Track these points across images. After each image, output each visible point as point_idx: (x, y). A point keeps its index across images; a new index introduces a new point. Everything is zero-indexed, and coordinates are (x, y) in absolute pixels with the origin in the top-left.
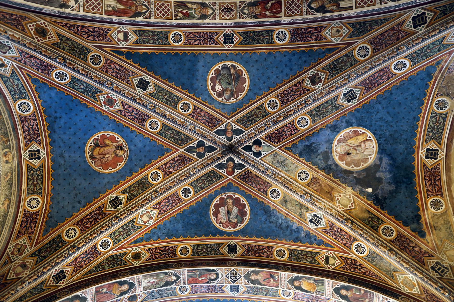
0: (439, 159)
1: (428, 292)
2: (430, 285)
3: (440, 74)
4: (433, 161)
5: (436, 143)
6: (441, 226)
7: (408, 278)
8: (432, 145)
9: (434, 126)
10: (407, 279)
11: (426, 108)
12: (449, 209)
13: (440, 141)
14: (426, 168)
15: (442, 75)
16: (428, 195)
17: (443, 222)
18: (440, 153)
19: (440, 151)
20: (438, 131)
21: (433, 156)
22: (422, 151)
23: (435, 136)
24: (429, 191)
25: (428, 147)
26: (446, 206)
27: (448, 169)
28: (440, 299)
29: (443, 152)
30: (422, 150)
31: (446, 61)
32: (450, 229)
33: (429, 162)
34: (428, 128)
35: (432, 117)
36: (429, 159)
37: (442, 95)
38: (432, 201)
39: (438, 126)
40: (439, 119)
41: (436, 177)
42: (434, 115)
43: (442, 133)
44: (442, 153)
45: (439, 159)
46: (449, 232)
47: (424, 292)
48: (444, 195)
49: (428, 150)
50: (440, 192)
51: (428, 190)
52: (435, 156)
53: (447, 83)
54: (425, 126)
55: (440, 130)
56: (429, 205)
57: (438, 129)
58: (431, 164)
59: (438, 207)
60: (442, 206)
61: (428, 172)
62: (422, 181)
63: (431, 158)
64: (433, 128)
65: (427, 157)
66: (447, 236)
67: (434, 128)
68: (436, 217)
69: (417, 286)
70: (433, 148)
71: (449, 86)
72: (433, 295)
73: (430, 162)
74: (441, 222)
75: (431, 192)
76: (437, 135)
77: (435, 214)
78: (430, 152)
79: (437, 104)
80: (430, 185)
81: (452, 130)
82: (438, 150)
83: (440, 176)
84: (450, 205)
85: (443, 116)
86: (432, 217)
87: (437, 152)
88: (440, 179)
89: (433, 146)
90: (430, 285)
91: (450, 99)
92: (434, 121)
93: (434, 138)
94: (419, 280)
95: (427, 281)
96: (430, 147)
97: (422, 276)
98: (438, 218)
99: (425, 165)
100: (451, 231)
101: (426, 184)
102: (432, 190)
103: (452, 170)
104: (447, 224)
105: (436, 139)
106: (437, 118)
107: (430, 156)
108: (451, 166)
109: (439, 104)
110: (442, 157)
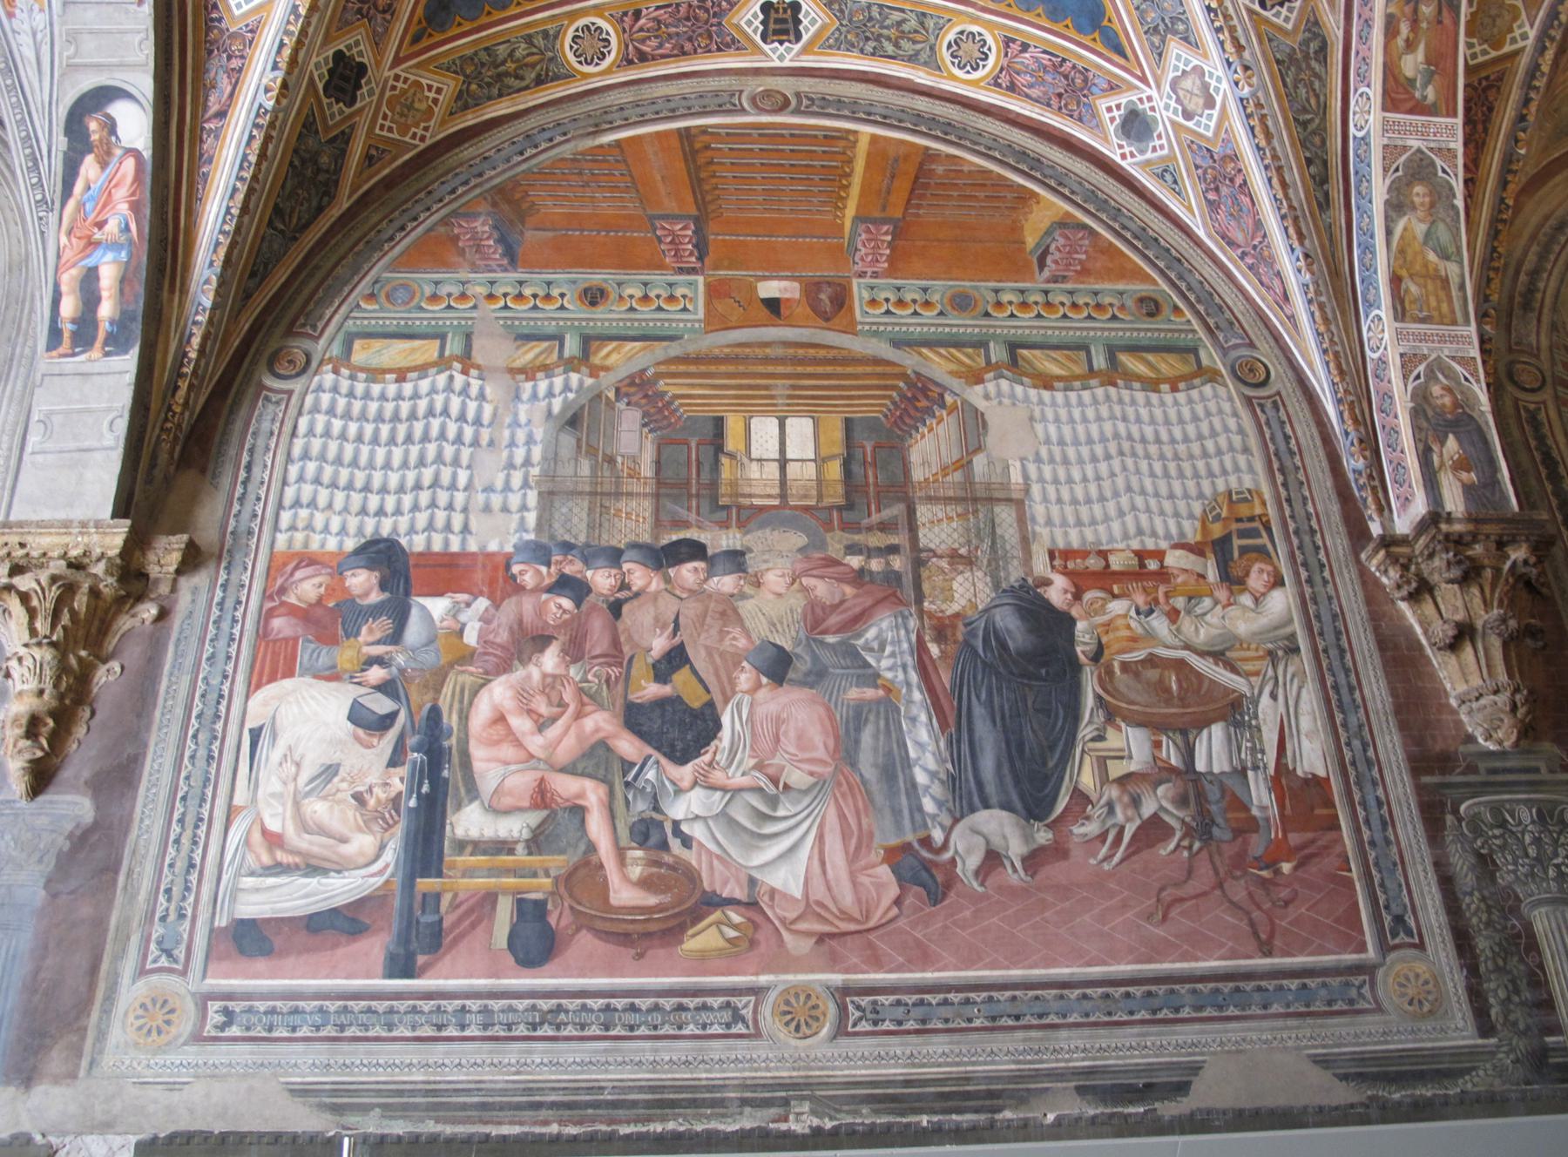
1: (1491, 94)
2: (1527, 101)
7: (1515, 18)
10: (1507, 17)
28: (1486, 130)
47: (1487, 78)
69: (1494, 54)
72: (1490, 109)
90: (1527, 101)
94: (1524, 61)
95: (1537, 88)
97: (1545, 68)
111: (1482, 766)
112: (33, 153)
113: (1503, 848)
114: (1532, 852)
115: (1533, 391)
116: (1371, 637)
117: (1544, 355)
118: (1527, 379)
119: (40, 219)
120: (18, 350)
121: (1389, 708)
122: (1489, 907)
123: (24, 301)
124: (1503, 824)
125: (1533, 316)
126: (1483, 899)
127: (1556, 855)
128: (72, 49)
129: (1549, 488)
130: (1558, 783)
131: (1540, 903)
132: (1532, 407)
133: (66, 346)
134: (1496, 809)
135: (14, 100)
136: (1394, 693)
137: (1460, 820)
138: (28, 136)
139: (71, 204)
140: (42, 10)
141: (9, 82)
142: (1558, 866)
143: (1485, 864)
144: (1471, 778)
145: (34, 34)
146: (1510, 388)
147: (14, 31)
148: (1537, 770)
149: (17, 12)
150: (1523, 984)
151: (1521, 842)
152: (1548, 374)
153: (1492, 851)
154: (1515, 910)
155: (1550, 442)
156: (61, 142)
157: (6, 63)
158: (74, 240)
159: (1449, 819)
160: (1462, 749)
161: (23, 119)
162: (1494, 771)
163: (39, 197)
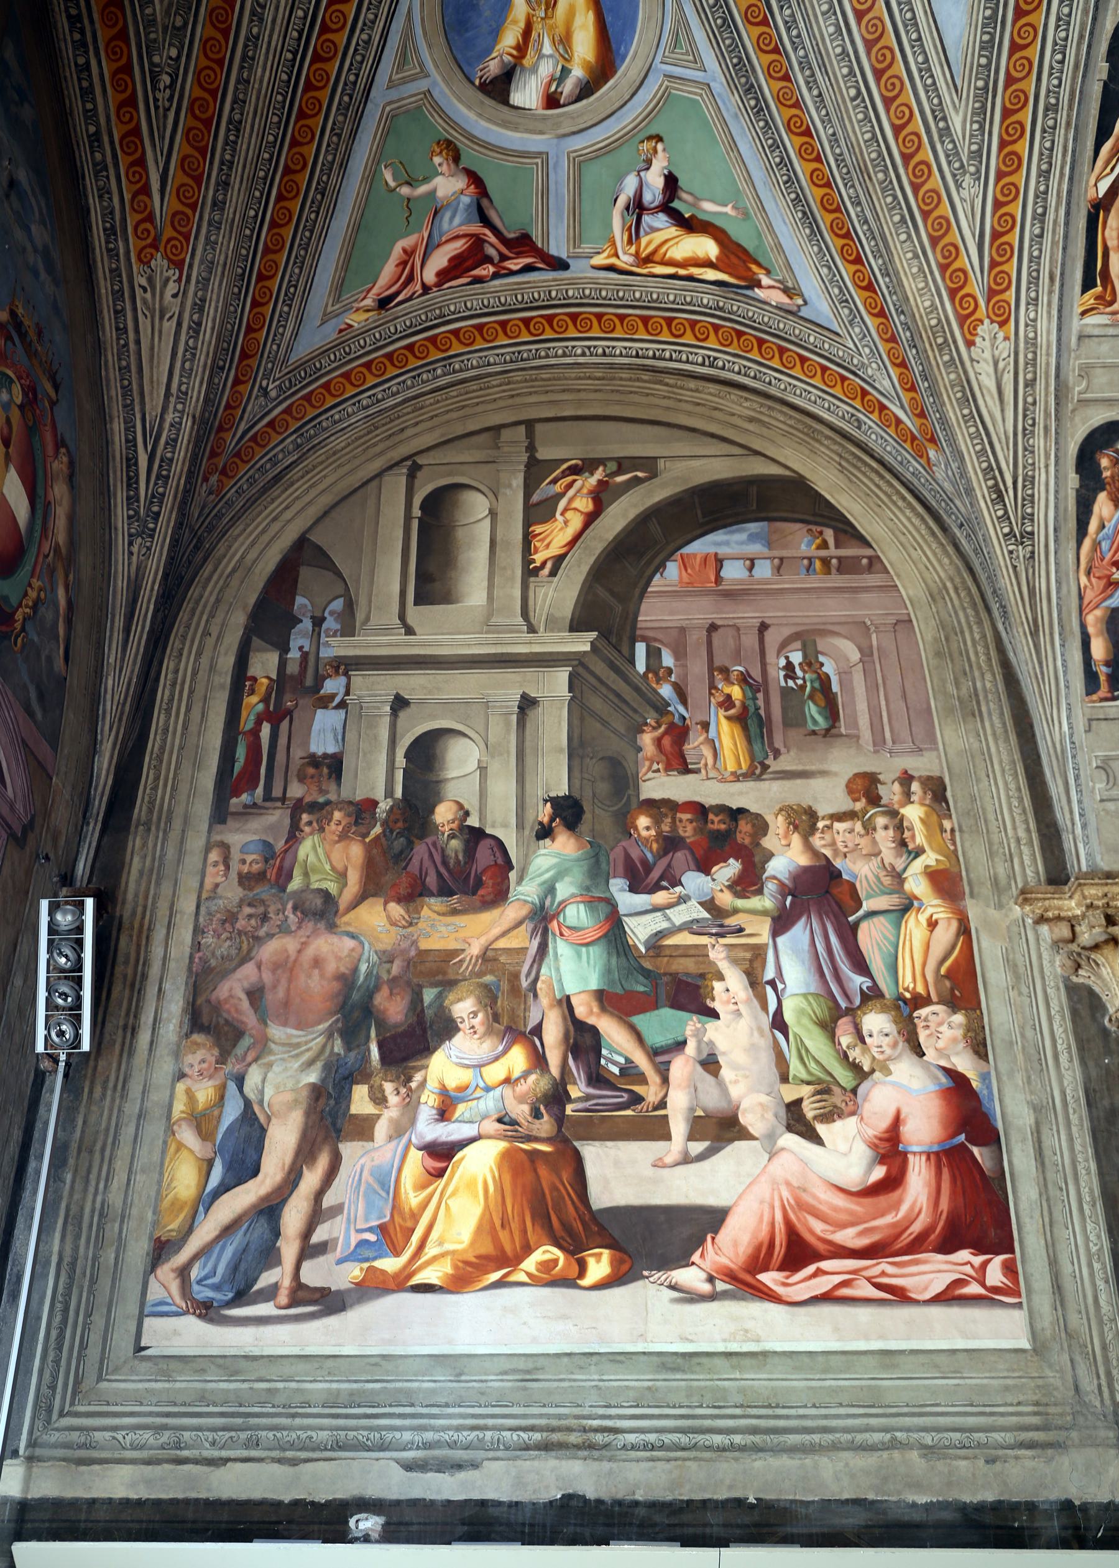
112: (996, 485)
119: (1011, 552)
120: (979, 685)
123: (962, 632)
128: (1084, 384)
133: (1104, 691)
135: (972, 430)
138: (990, 466)
139: (1087, 543)
140: (1007, 338)
141: (966, 412)
145: (996, 364)
147: (972, 360)
149: (978, 340)
156: (1073, 480)
157: (963, 391)
158: (1093, 580)
161: (984, 449)
163: (1006, 530)
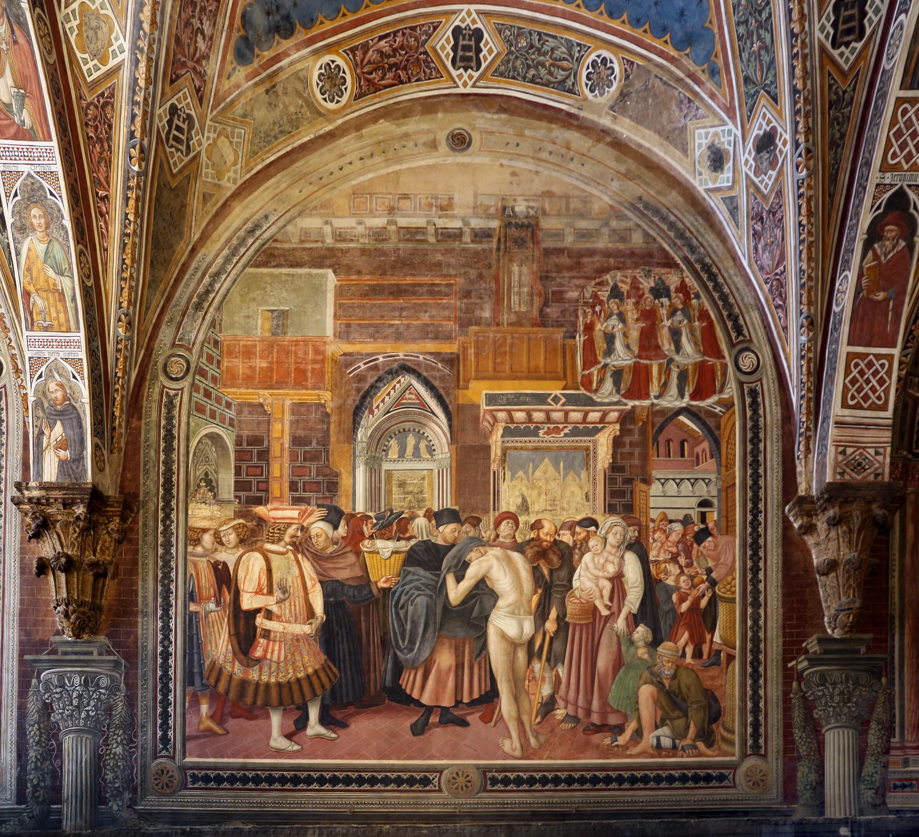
0: (454, 73)
3: (681, 75)
4: (448, 55)
5: (498, 62)
6: (281, 106)
8: (491, 47)
9: (545, 54)
11: (597, 26)
12: (330, 121)
13: (501, 75)
14: (426, 33)
15: (679, 80)
16: (353, 50)
17: (292, 109)
18: (471, 77)
19: (476, 75)
20: (529, 67)
21: (460, 53)
22: (474, 15)
23: (517, 58)
24: (365, 53)
25: (486, 35)
26: (335, 112)
27: (429, 106)
29: (474, 86)
30: (479, 13)
31: (712, 96)
32: (281, 132)
33: (443, 41)
34: (539, 34)
35: (569, 45)
36: (452, 42)
37: (627, 77)
38: (338, 66)
39: (543, 65)
40: (564, 69)
41: (405, 68)
42: (575, 52)
43: (524, 78)
44: (470, 83)
45: (454, 73)
46: (273, 133)
48: (362, 102)
49: (478, 35)
50: (368, 87)
51: (365, 47)
52: (464, 59)
53: (655, 95)
54: (546, 23)
55: (532, 72)
56: (327, 58)
57: (536, 67)
58: (438, 47)
59: (327, 87)
60: (332, 101)
61: (417, 40)
62: (387, 24)
63: (455, 49)
64: (539, 50)
65: (457, 32)
66: (263, 129)
67: (539, 55)
68: (300, 87)
70: (485, 51)
71: (645, 100)
73: (443, 44)
74: (292, 104)
75: (362, 61)
76: (519, 62)
77: (305, 81)
78: (473, 43)
79: (604, 60)
80: (380, 52)
81: (530, 108)
82: (478, 70)
83: (409, 81)
84: (340, 122)
85: (569, 83)
86: (296, 75)
87: (473, 64)
88: (401, 82)
89: (490, 51)
91: (611, 103)
92: (558, 54)
93: (510, 53)
96: (487, 43)
98: (300, 95)
99: (435, 28)
100: (276, 138)
101: (381, 38)
102: (369, 62)
103: (429, 117)
104: (290, 121)
105: (508, 61)
106: (565, 63)
107: (461, 43)
108: (440, 115)
109: (602, 67)
110: (460, 83)
111: (61, 649)
113: (59, 699)
114: (75, 702)
115: (177, 379)
116: (17, 565)
117: (196, 349)
118: (175, 371)
121: (17, 612)
122: (41, 733)
124: (63, 686)
125: (201, 314)
126: (39, 729)
127: (88, 705)
129: (162, 457)
130: (102, 661)
131: (70, 732)
132: (172, 393)
134: (61, 677)
136: (22, 602)
137: (39, 682)
142: (88, 711)
143: (47, 709)
144: (52, 657)
146: (162, 378)
148: (91, 653)
150: (48, 777)
151: (70, 696)
152: (193, 365)
153: (52, 701)
154: (55, 736)
155: (175, 422)
159: (34, 681)
160: (52, 639)
162: (66, 653)
